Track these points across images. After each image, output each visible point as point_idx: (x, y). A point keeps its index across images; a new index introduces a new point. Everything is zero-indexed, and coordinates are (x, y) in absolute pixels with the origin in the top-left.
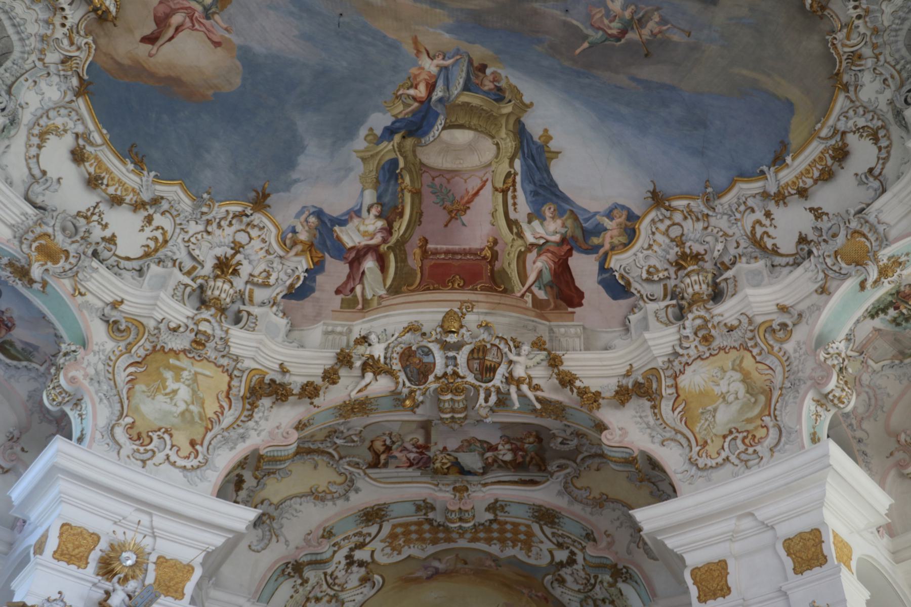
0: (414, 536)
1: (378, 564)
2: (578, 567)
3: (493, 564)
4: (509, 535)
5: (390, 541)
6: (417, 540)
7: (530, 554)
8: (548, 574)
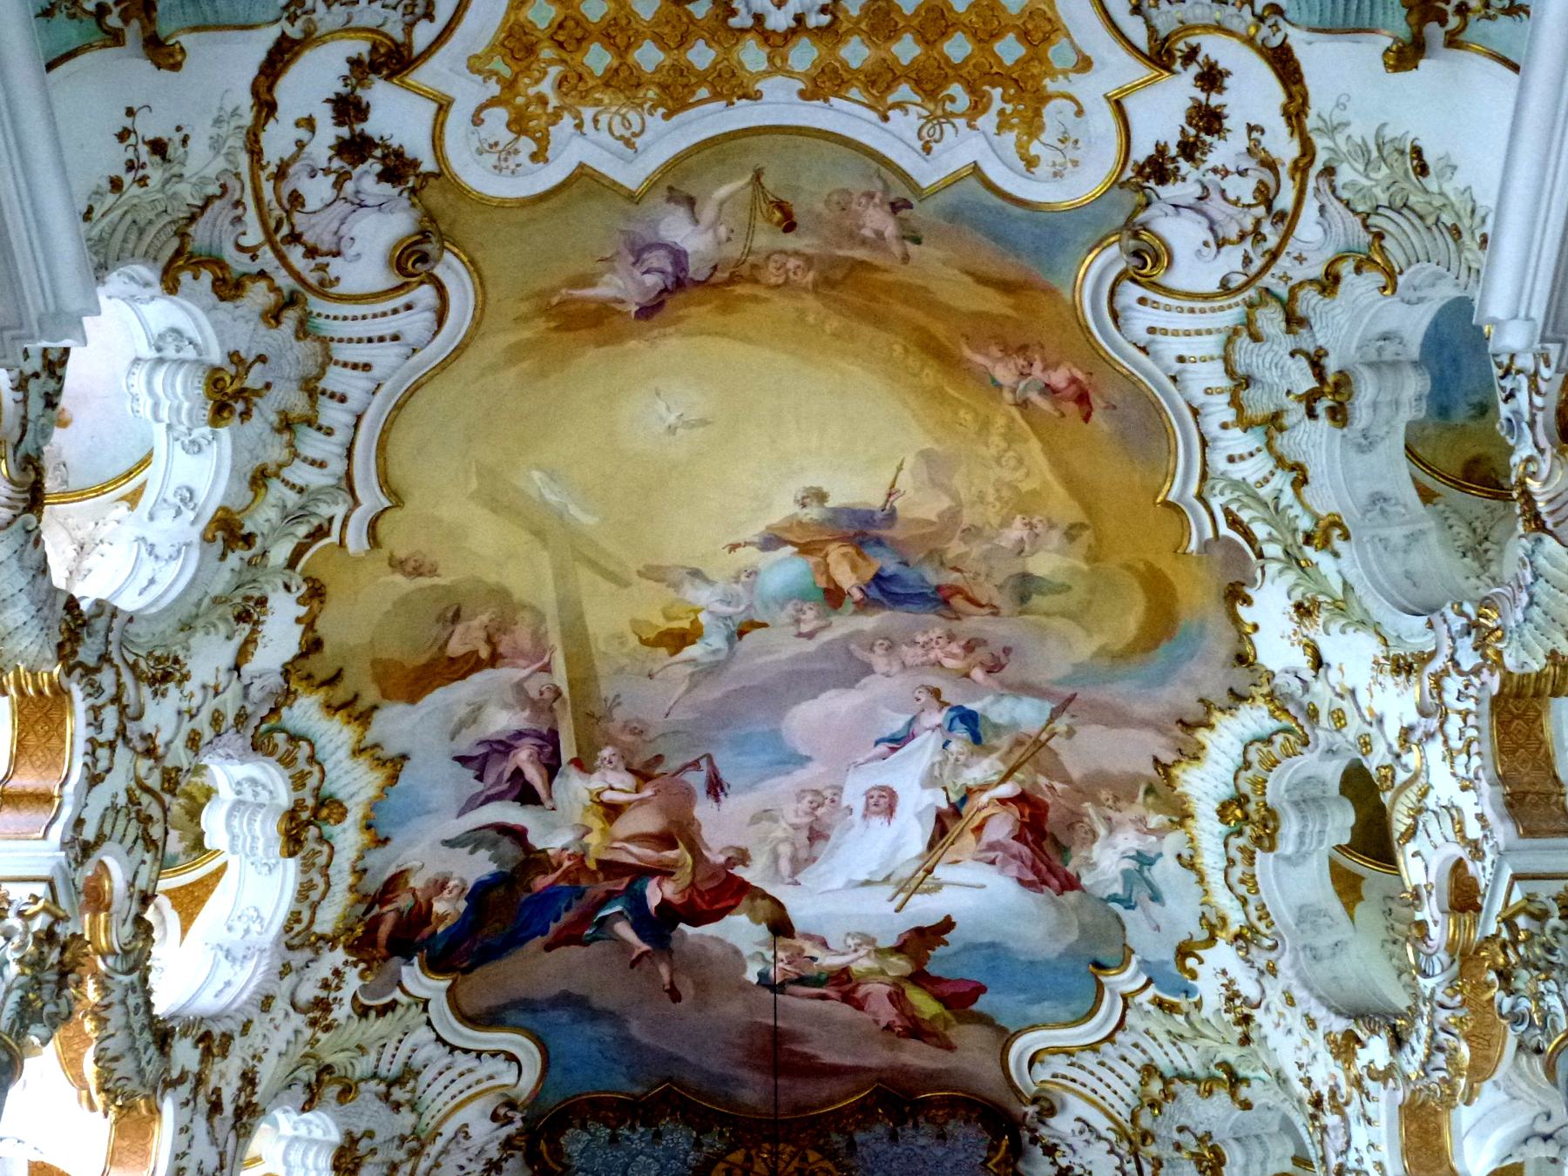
0: (598, 58)
1: (461, 191)
2: (1225, 151)
3: (890, 229)
4: (957, 48)
5: (507, 72)
6: (610, 80)
7: (1035, 148)
8: (1100, 244)
